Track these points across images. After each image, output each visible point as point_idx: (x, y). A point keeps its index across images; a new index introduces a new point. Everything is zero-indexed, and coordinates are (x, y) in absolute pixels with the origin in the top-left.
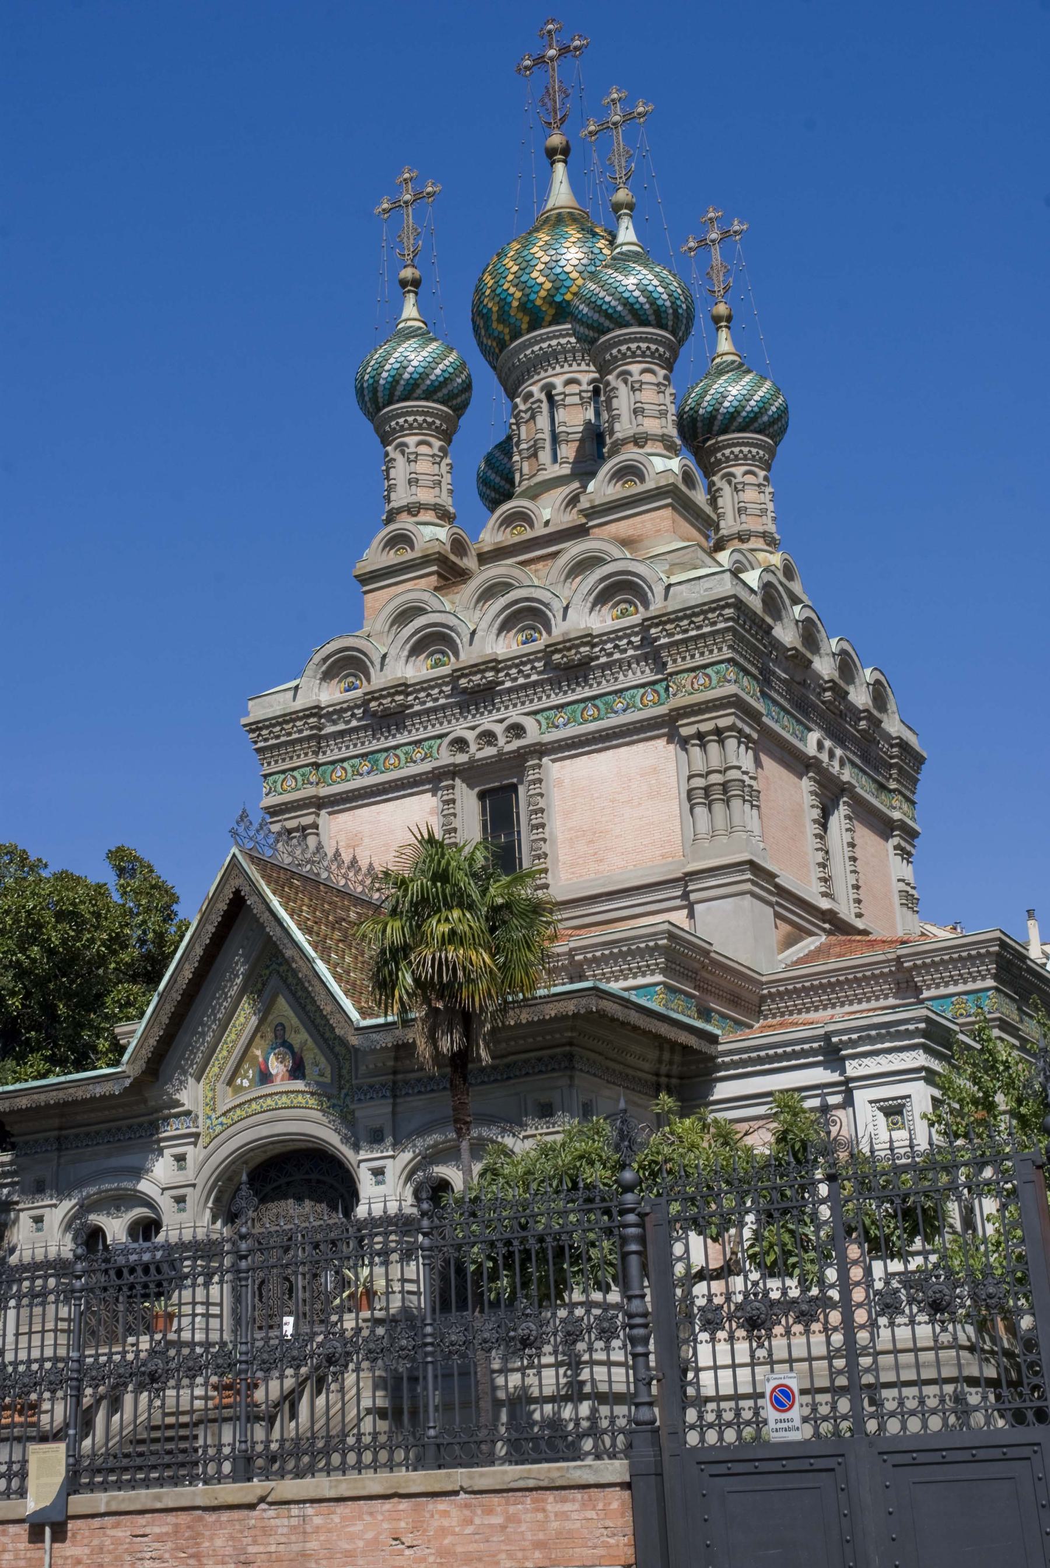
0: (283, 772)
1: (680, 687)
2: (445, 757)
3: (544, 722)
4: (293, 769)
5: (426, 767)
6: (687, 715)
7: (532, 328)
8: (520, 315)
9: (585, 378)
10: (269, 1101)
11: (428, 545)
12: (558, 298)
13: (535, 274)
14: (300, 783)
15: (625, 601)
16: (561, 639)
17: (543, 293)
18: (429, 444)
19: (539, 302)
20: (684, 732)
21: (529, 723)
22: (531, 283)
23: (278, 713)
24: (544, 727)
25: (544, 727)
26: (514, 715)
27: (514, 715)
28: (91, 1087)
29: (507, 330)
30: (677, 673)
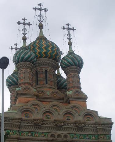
4: (13, 130)
5: (45, 138)
8: (44, 54)
12: (52, 54)
13: (49, 48)
14: (14, 133)
16: (79, 121)
17: (50, 52)
19: (48, 53)
21: (68, 135)
22: (48, 49)
23: (12, 117)
24: (71, 137)
25: (71, 137)
26: (65, 133)
27: (65, 133)
29: (54, 58)
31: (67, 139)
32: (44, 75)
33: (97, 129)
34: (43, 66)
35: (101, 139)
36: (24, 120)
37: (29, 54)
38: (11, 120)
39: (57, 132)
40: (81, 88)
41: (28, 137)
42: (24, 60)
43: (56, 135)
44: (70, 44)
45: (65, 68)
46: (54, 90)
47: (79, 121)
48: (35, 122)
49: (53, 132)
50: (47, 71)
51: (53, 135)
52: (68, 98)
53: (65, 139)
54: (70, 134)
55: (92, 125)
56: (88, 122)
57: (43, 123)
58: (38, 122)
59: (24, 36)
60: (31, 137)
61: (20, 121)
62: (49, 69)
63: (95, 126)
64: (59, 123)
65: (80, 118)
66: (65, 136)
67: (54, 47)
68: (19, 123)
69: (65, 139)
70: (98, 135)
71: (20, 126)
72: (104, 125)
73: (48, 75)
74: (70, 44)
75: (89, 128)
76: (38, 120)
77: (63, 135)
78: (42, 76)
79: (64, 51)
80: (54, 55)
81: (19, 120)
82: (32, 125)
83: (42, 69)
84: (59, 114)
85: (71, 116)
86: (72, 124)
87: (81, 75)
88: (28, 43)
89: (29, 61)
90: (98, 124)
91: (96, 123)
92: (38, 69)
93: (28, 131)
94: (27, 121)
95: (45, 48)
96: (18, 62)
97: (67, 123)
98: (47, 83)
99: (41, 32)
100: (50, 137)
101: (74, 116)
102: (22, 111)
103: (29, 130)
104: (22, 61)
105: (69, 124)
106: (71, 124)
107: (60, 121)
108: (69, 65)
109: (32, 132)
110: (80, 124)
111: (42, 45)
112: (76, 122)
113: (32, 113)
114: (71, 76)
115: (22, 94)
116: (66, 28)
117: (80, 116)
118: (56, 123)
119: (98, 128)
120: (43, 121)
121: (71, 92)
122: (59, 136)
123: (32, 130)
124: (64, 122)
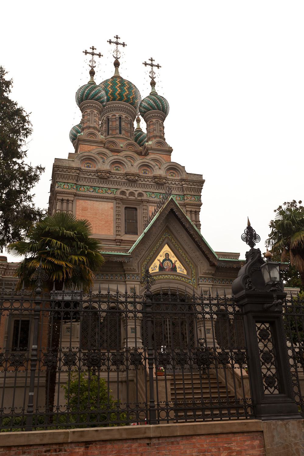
0: (64, 183)
1: (187, 198)
2: (118, 195)
3: (148, 195)
4: (68, 183)
5: (112, 195)
6: (188, 205)
7: (119, 100)
8: (118, 96)
9: (129, 118)
10: (166, 276)
11: (102, 139)
12: (129, 96)
15: (173, 173)
17: (126, 93)
18: (99, 115)
19: (124, 95)
20: (188, 209)
21: (144, 193)
23: (67, 166)
26: (140, 190)
27: (140, 190)
28: (115, 258)
30: (187, 195)
31: (142, 198)
32: (118, 123)
33: (183, 187)
34: (117, 112)
35: (187, 200)
36: (84, 170)
37: (96, 89)
38: (66, 170)
39: (129, 188)
40: (165, 139)
41: (88, 193)
42: (89, 97)
43: (128, 192)
44: (153, 84)
45: (145, 112)
46: (130, 141)
47: (160, 175)
48: (98, 173)
49: (123, 188)
50: (122, 117)
51: (123, 193)
52: (147, 150)
53: (139, 198)
54: (146, 192)
55: (176, 183)
56: (171, 177)
57: (110, 176)
58: (103, 174)
59: (92, 69)
60: (93, 194)
61: (79, 171)
62: (124, 116)
63: (180, 183)
64: (133, 177)
65: (160, 172)
66: (140, 195)
67: (131, 86)
68: (77, 174)
69: (139, 198)
70: (184, 195)
71: (78, 178)
72: (193, 182)
73: (123, 124)
74: (153, 84)
75: (172, 185)
76: (103, 171)
77: (136, 193)
78: (114, 124)
79: (144, 92)
80: (131, 97)
81: (77, 170)
82: (95, 177)
83: (115, 115)
84: (132, 165)
85: (148, 169)
86: (150, 180)
87: (165, 124)
88: (98, 80)
89: (97, 100)
90: (184, 181)
91: (182, 180)
92: (110, 116)
93: (89, 186)
94: (89, 172)
95: (120, 87)
96: (82, 101)
97: (144, 178)
98: (120, 133)
99: (117, 71)
100: (119, 194)
101: (153, 169)
102: (82, 159)
103: (90, 184)
104: (86, 99)
105: (146, 180)
106: (149, 180)
107: (133, 175)
108: (150, 108)
109: (94, 186)
110: (160, 179)
111: (116, 84)
112: (155, 177)
113: (96, 161)
114: (152, 123)
115: (85, 141)
116: (149, 64)
117: (160, 170)
118: (128, 177)
119: (183, 186)
120: (109, 172)
121: (150, 143)
122: (132, 194)
123: (95, 184)
124: (139, 176)
